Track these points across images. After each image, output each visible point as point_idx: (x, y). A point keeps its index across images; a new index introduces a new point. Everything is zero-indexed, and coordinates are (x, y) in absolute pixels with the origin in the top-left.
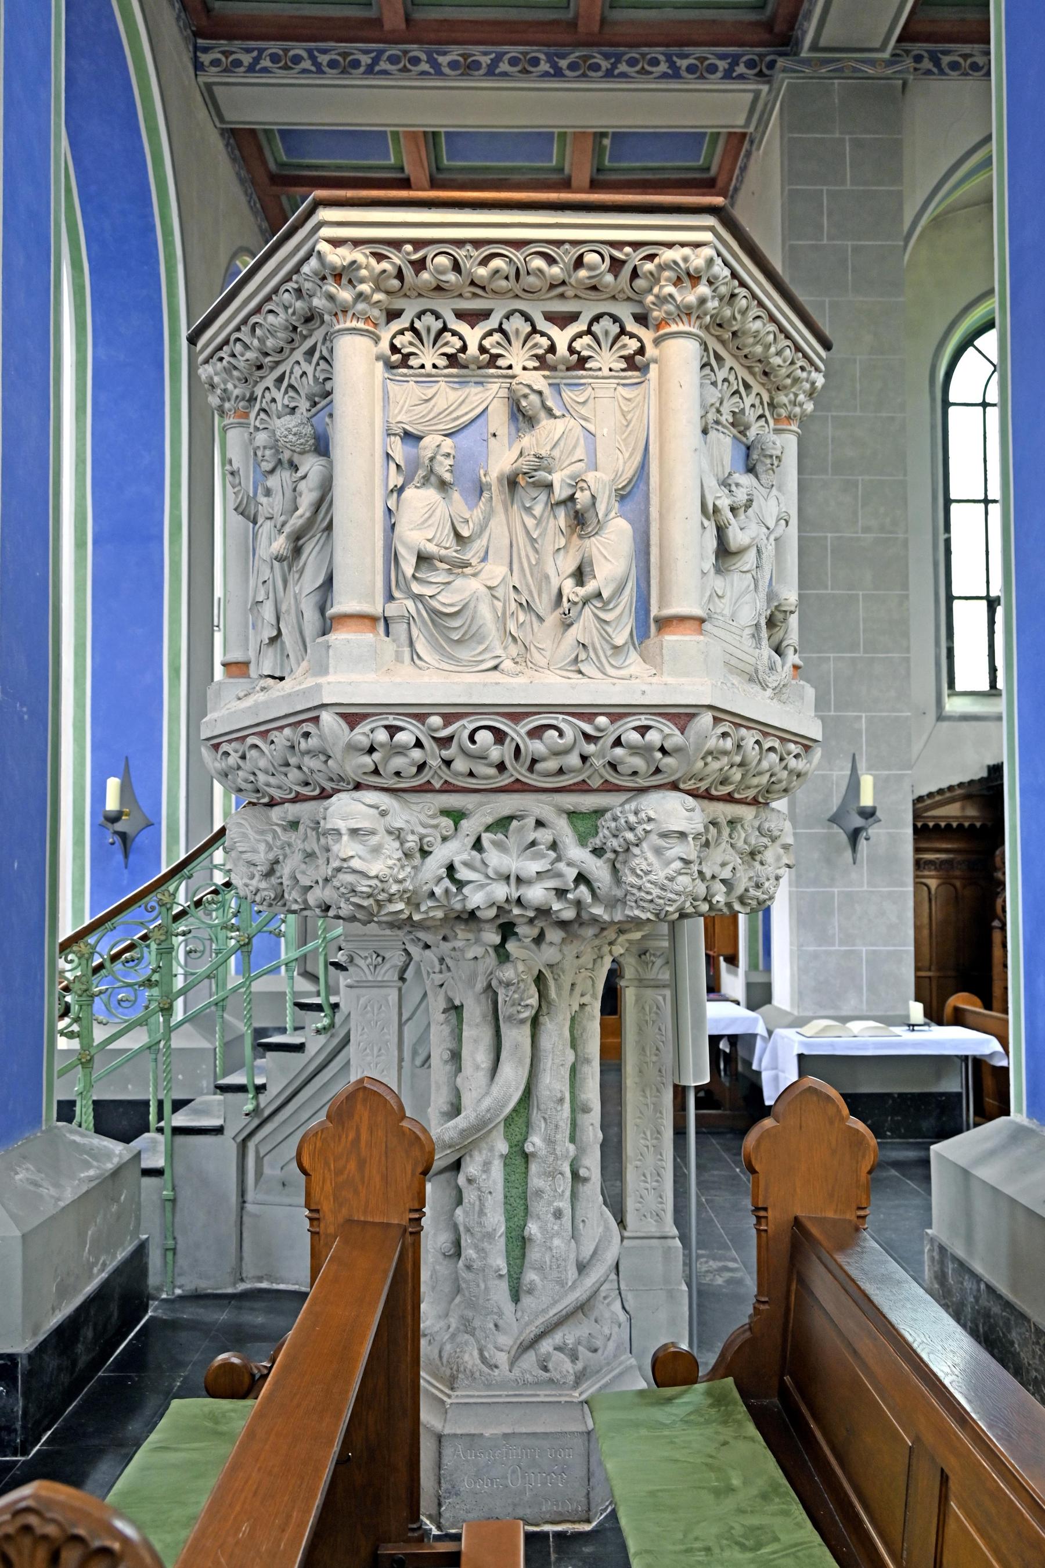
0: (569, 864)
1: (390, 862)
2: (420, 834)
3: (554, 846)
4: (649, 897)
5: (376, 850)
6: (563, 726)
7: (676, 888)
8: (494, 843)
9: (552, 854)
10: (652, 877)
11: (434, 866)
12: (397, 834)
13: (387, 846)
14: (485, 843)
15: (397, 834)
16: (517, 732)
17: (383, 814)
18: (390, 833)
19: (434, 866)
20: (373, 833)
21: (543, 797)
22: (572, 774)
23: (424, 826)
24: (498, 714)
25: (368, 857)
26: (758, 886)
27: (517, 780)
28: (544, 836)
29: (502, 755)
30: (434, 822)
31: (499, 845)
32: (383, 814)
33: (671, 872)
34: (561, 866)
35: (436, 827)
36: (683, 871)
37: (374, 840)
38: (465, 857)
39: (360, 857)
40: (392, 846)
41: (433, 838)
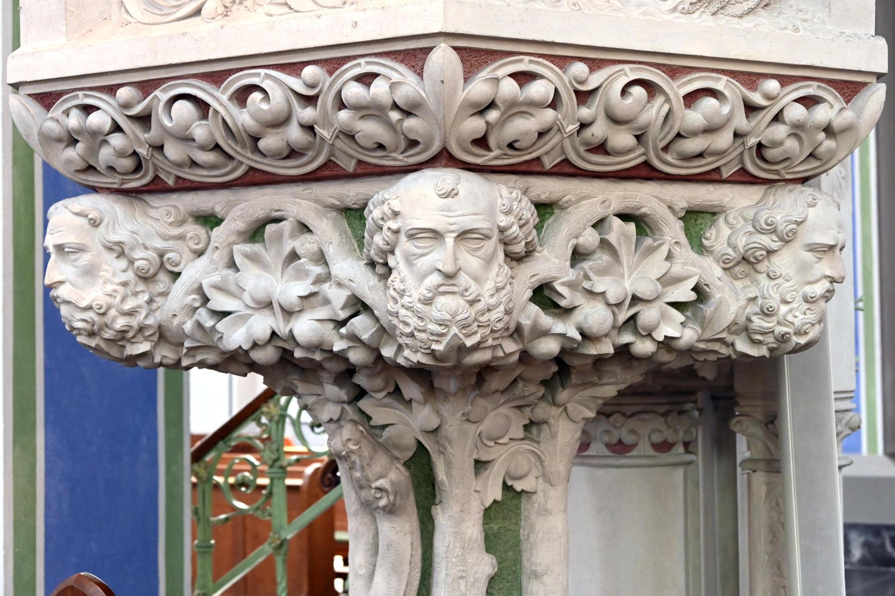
0: (340, 285)
1: (110, 288)
2: (156, 250)
3: (321, 258)
4: (408, 330)
5: (90, 272)
6: (266, 85)
7: (437, 315)
8: (249, 257)
9: (318, 270)
10: (406, 300)
11: (179, 295)
12: (119, 250)
13: (105, 267)
14: (238, 260)
15: (119, 250)
16: (219, 98)
17: (95, 224)
18: (110, 249)
19: (179, 295)
20: (80, 249)
21: (299, 189)
22: (710, 159)
23: (166, 238)
24: (195, 76)
25: (80, 281)
26: (767, 313)
27: (251, 169)
28: (305, 245)
29: (211, 134)
30: (176, 231)
31: (254, 258)
32: (95, 224)
33: (425, 292)
34: (327, 289)
35: (181, 238)
36: (442, 289)
37: (85, 259)
38: (216, 278)
39: (71, 283)
40: (114, 270)
41: (177, 253)
